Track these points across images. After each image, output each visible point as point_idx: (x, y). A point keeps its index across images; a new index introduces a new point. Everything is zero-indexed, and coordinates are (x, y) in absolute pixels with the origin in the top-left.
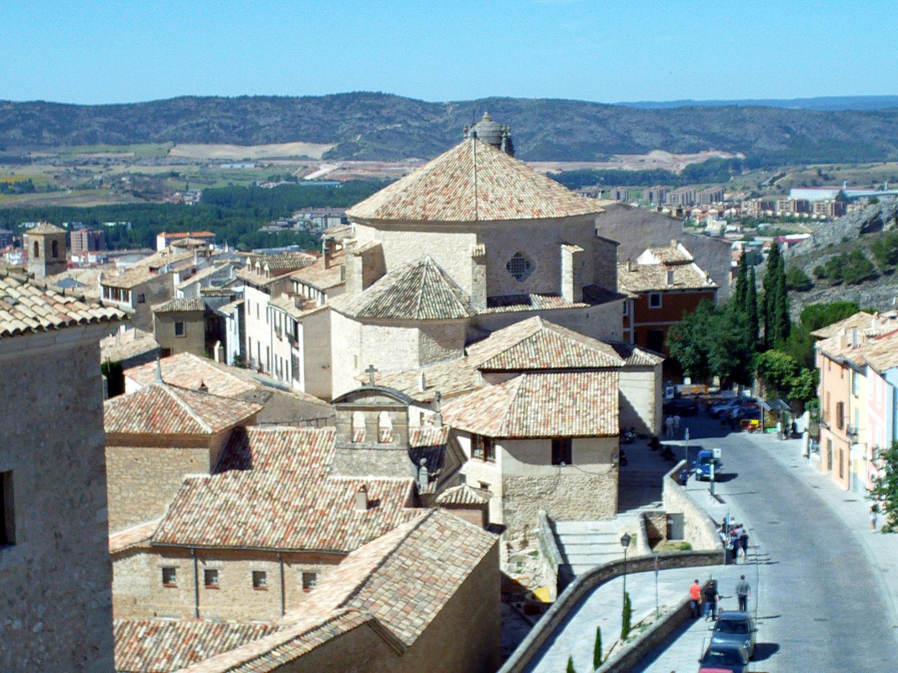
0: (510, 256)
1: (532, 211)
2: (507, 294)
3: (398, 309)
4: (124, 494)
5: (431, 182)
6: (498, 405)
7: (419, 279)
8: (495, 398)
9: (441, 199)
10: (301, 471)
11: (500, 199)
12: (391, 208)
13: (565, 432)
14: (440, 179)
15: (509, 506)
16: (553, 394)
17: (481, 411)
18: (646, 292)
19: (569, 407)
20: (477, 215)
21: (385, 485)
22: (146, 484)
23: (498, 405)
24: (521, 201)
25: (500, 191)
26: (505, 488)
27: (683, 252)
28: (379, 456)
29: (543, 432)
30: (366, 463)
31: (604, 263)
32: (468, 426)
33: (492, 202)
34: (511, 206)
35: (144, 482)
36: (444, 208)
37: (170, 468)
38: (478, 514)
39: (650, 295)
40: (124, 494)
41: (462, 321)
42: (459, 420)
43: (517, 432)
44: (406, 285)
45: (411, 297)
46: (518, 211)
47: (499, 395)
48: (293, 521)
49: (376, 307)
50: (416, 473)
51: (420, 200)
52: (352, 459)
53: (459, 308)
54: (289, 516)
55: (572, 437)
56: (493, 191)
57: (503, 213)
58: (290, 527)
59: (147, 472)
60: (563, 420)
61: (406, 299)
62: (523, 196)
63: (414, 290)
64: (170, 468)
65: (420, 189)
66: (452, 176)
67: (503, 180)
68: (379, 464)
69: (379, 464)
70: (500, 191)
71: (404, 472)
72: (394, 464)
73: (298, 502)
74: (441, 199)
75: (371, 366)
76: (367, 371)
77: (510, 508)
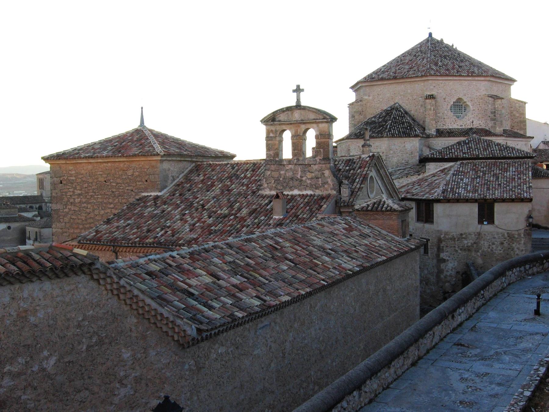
1: (468, 72)
2: (451, 127)
4: (96, 212)
7: (390, 116)
8: (435, 178)
9: (407, 67)
17: (424, 186)
19: (493, 181)
21: (308, 198)
22: (111, 203)
28: (304, 171)
30: (292, 179)
32: (413, 195)
33: (440, 66)
35: (111, 201)
36: (408, 71)
37: (129, 188)
38: (395, 222)
40: (96, 212)
42: (408, 193)
44: (380, 120)
45: (383, 125)
47: (438, 176)
49: (360, 132)
50: (337, 187)
51: (393, 70)
52: (280, 174)
53: (415, 131)
56: (441, 61)
59: (113, 192)
60: (488, 189)
61: (380, 127)
63: (386, 122)
64: (129, 188)
66: (415, 56)
67: (448, 56)
68: (304, 179)
69: (304, 179)
70: (446, 61)
71: (326, 186)
72: (318, 178)
73: (225, 211)
74: (407, 67)
75: (298, 86)
76: (294, 91)
77: (444, 258)
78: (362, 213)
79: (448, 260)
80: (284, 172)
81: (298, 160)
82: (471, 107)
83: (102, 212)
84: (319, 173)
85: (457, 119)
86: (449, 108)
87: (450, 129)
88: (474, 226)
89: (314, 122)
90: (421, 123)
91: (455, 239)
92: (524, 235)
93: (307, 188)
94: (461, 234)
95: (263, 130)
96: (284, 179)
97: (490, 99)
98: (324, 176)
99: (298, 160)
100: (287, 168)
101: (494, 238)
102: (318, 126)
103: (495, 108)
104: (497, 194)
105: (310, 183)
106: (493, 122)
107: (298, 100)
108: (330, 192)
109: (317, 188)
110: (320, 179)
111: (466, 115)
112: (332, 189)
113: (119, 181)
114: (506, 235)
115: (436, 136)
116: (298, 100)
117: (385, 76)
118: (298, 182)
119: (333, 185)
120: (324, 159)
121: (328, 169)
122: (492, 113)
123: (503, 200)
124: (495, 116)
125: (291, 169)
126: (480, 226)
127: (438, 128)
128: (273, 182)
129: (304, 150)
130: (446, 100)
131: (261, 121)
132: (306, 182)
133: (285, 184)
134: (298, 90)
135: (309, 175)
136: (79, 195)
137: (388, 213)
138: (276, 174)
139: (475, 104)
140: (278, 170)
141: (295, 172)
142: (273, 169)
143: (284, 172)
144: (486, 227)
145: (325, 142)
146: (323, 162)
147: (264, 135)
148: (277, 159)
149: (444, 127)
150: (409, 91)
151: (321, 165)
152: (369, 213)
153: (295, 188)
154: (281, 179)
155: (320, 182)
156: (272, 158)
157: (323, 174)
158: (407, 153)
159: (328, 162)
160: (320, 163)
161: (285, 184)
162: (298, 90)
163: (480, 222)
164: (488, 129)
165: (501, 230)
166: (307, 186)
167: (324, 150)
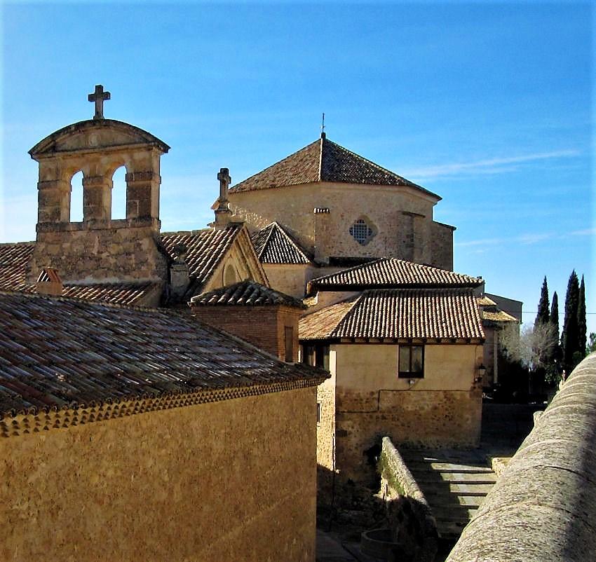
0: (353, 219)
5: (283, 166)
26: (339, 403)
28: (104, 243)
30: (83, 256)
31: (441, 245)
52: (61, 248)
53: (301, 256)
68: (104, 255)
69: (104, 255)
72: (128, 254)
76: (91, 98)
78: (207, 309)
79: (350, 433)
80: (69, 244)
81: (95, 220)
82: (378, 227)
84: (132, 244)
85: (359, 245)
86: (348, 229)
88: (394, 381)
89: (127, 147)
90: (309, 248)
91: (362, 400)
92: (471, 396)
93: (111, 272)
94: (372, 393)
95: (32, 170)
96: (68, 257)
97: (406, 217)
98: (141, 250)
99: (95, 220)
100: (75, 237)
101: (424, 399)
102: (131, 157)
103: (412, 229)
104: (429, 332)
105: (116, 263)
106: (409, 249)
107: (99, 112)
108: (150, 278)
109: (127, 272)
110: (133, 256)
111: (372, 240)
112: (153, 274)
115: (330, 265)
116: (99, 112)
117: (260, 185)
118: (93, 262)
119: (157, 266)
120: (141, 218)
121: (147, 236)
122: (408, 236)
123: (438, 341)
124: (412, 240)
125: (81, 239)
127: (332, 256)
128: (49, 263)
129: (105, 203)
130: (344, 218)
131: (30, 152)
132: (107, 261)
133: (70, 267)
134: (99, 95)
137: (258, 308)
138: (54, 250)
139: (385, 225)
140: (58, 242)
141: (87, 243)
142: (50, 241)
143: (69, 244)
145: (143, 186)
146: (140, 223)
147: (36, 179)
148: (57, 221)
149: (341, 256)
150: (292, 205)
151: (136, 229)
152: (220, 308)
153: (88, 272)
154: (63, 258)
155: (133, 261)
156: (49, 221)
157: (139, 245)
158: (288, 287)
159: (148, 223)
160: (133, 226)
161: (70, 267)
162: (99, 95)
166: (109, 269)
167: (141, 201)
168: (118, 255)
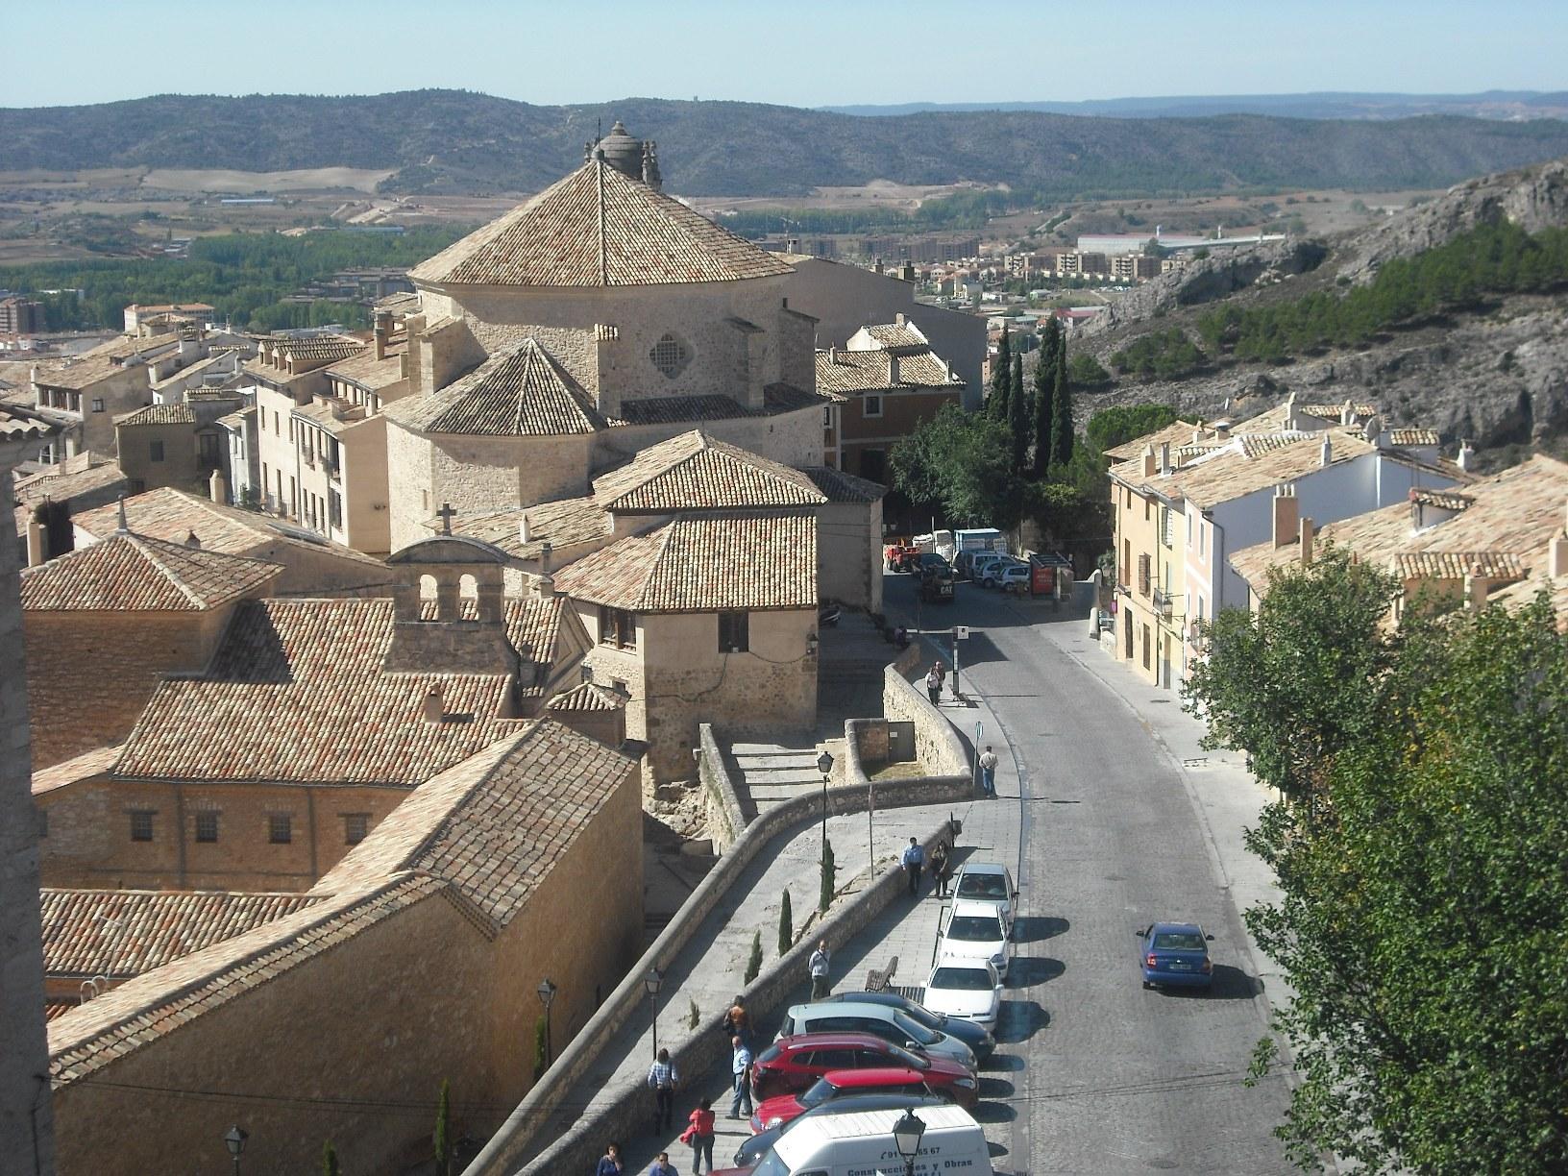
3: (487, 420)
5: (536, 227)
6: (639, 564)
8: (635, 553)
10: (341, 666)
11: (639, 254)
12: (476, 267)
13: (738, 602)
14: (549, 222)
15: (657, 712)
16: (720, 546)
18: (860, 392)
20: (605, 277)
22: (101, 690)
23: (639, 564)
24: (671, 256)
25: (640, 242)
27: (913, 333)
28: (459, 641)
29: (705, 602)
34: (657, 264)
35: (101, 685)
39: (864, 397)
41: (583, 438)
42: (581, 586)
43: (666, 602)
44: (499, 385)
46: (667, 272)
48: (330, 741)
54: (324, 732)
55: (748, 609)
57: (643, 275)
58: (325, 747)
62: (674, 248)
63: (511, 392)
65: (520, 237)
66: (567, 219)
70: (640, 242)
73: (337, 712)
83: (85, 704)
87: (650, 402)
88: (712, 656)
113: (117, 651)
114: (770, 671)
126: (722, 656)
135: (469, 648)
136: (34, 673)
144: (736, 657)
149: (639, 397)
163: (724, 648)
164: (731, 396)
165: (760, 663)
168: (472, 653)
